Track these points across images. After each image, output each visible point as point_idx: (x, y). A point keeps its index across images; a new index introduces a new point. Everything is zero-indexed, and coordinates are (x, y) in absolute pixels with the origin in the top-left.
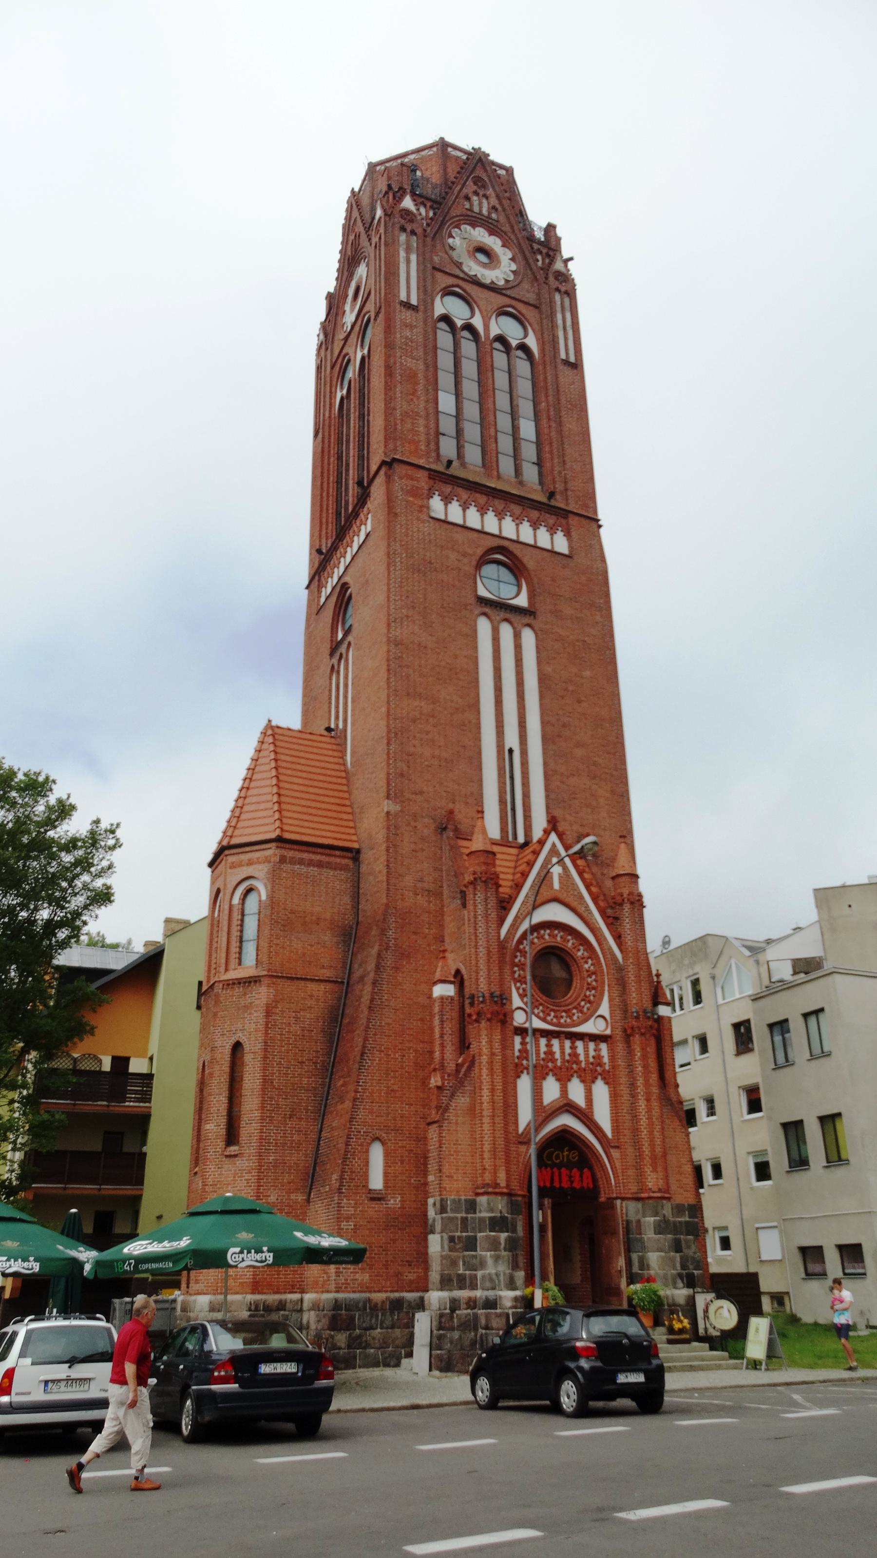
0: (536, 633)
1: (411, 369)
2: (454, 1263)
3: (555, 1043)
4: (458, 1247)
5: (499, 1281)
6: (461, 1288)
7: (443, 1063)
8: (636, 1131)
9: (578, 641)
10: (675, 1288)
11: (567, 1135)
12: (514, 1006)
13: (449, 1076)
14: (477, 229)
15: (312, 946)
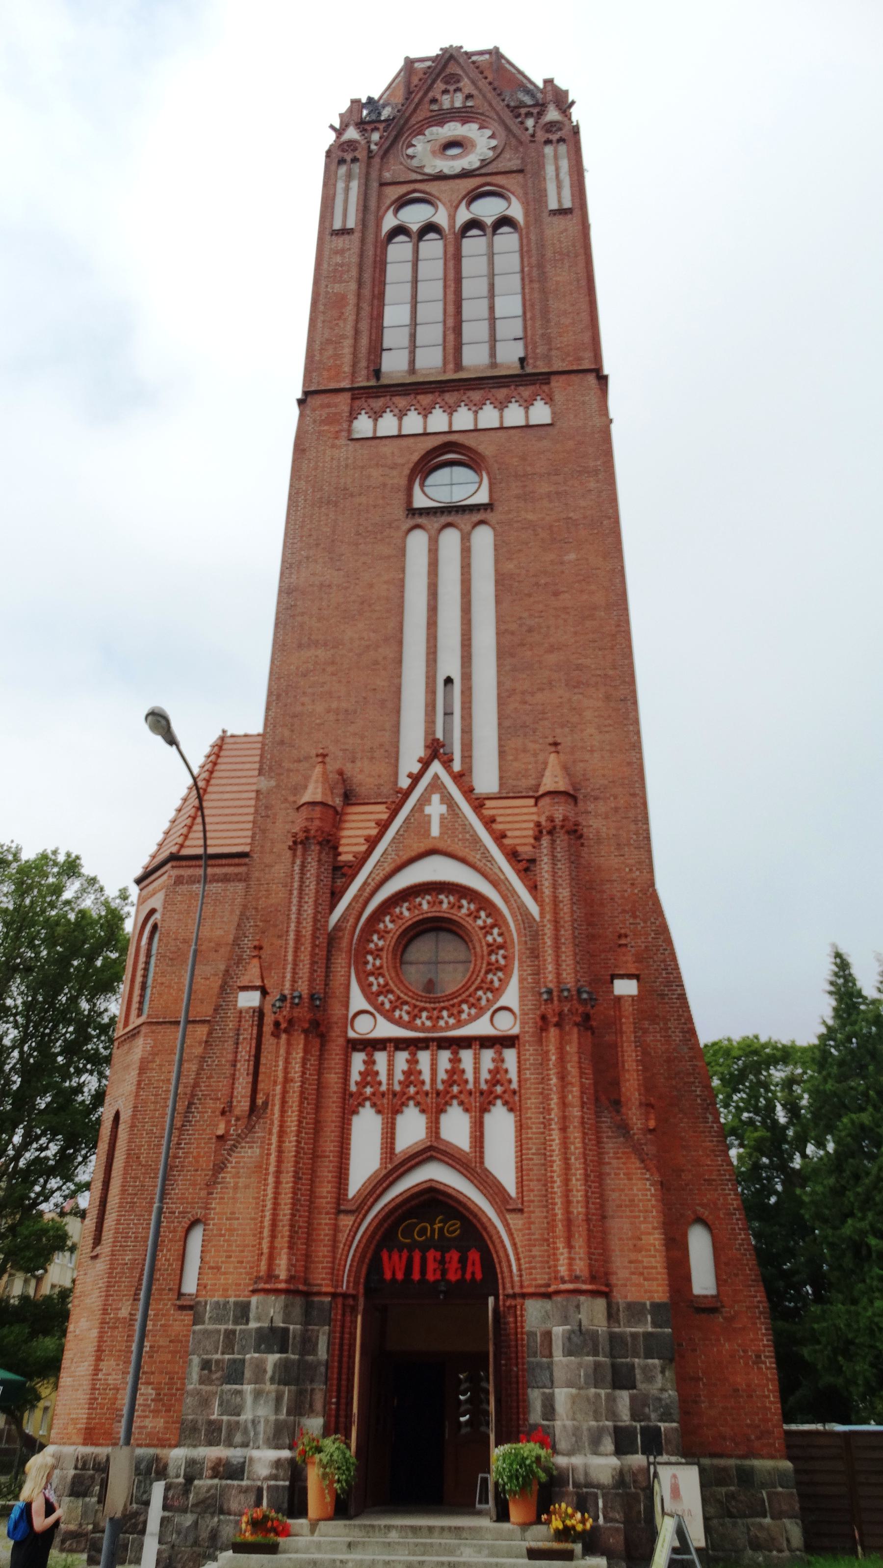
0: (494, 528)
1: (336, 294)
2: (205, 1402)
3: (424, 1057)
4: (214, 1377)
5: (256, 1434)
6: (210, 1443)
7: (231, 1102)
8: (546, 1182)
9: (558, 520)
10: (596, 1453)
11: (441, 1198)
12: (352, 1011)
13: (238, 1119)
14: (447, 126)
15: (207, 979)
